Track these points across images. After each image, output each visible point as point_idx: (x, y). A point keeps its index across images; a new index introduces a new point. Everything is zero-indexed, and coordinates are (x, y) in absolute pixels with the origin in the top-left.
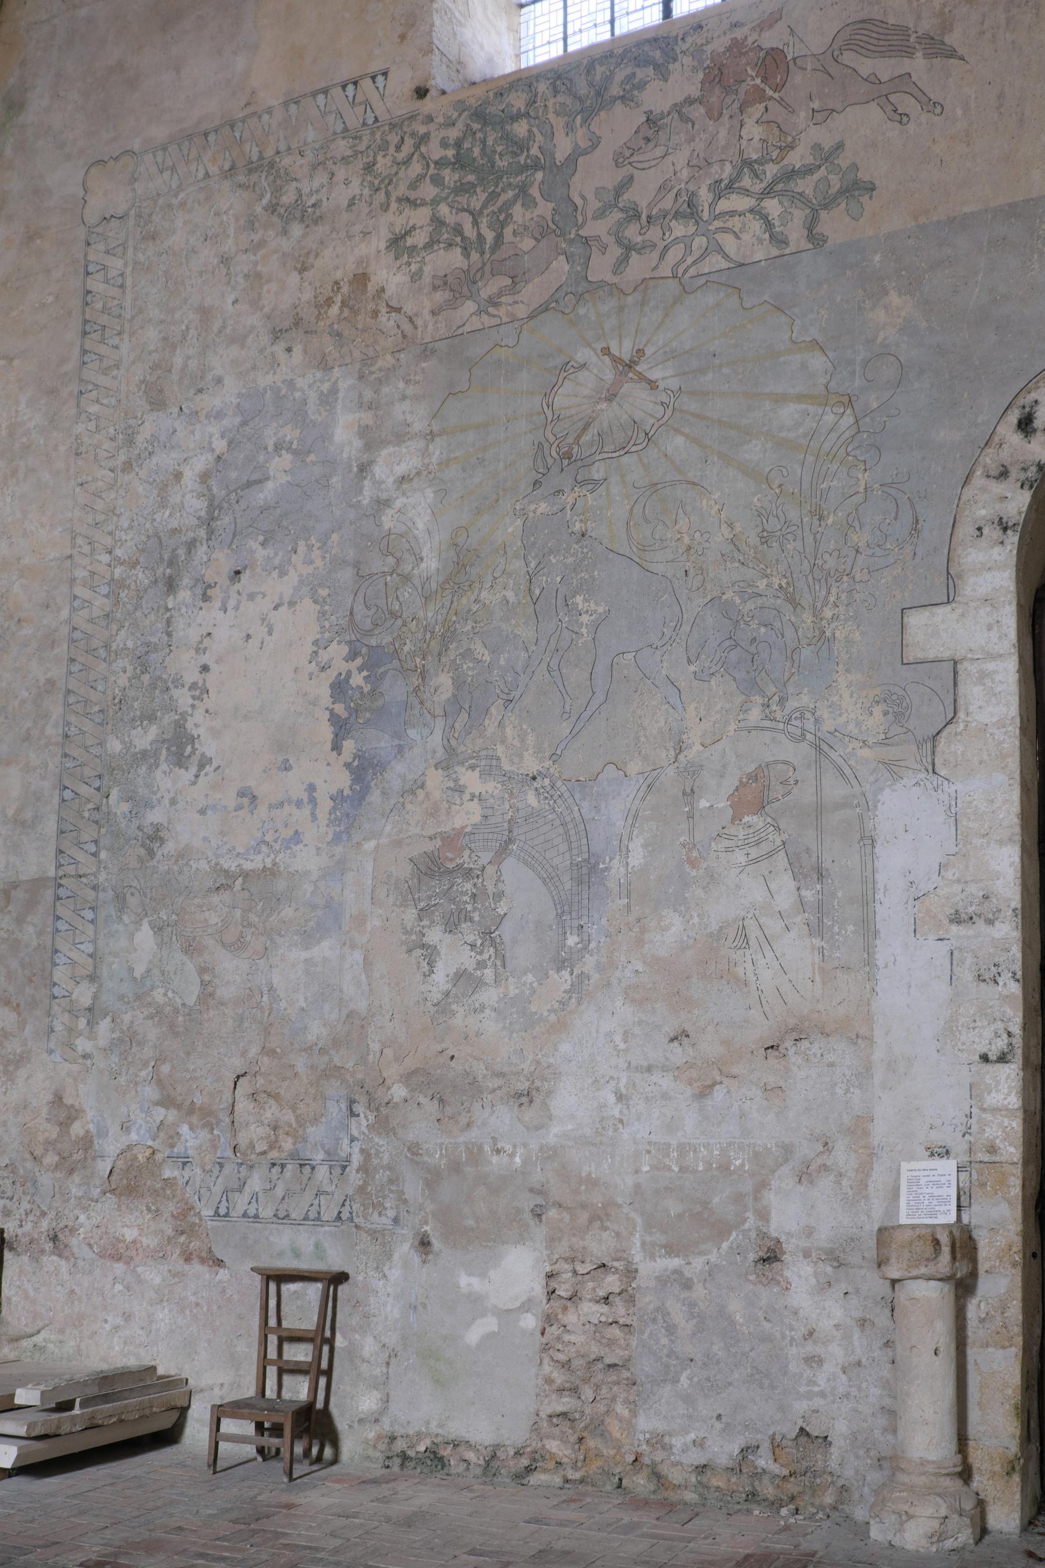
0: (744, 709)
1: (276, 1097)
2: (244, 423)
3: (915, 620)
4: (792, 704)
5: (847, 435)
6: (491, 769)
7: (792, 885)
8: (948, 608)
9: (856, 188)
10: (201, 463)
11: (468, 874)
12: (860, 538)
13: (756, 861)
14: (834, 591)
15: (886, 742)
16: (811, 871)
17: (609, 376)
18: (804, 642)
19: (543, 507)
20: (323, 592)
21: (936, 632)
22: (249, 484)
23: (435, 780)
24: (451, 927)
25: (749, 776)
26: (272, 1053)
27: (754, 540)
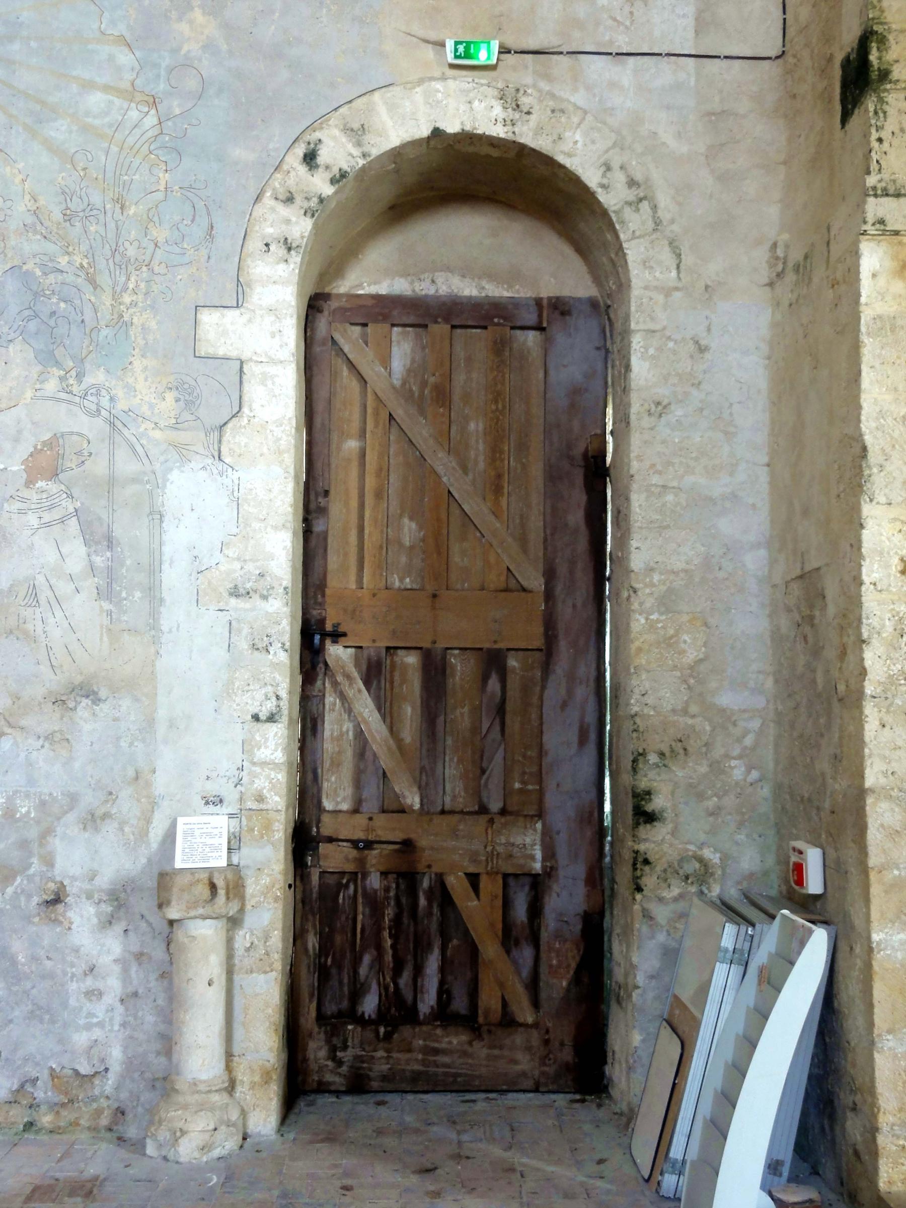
0: (42, 378)
3: (208, 318)
4: (89, 380)
5: (150, 134)
7: (83, 550)
8: (237, 312)
12: (161, 234)
13: (48, 525)
14: (133, 279)
16: (101, 539)
18: (103, 323)
21: (223, 331)
25: (44, 443)
27: (57, 216)
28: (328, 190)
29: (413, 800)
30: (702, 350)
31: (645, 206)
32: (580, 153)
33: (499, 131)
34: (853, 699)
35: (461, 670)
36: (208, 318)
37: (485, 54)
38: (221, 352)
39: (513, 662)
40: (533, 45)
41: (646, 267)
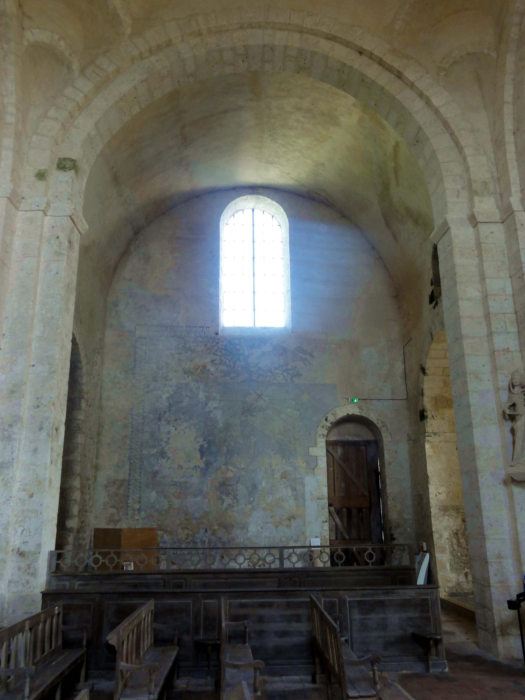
1: (187, 529)
2: (177, 389)
3: (310, 449)
4: (290, 460)
6: (235, 466)
9: (299, 375)
10: (167, 395)
11: (231, 485)
15: (306, 468)
17: (256, 397)
19: (244, 418)
20: (197, 427)
22: (179, 402)
23: (223, 467)
24: (227, 495)
26: (187, 519)
28: (330, 425)
29: (347, 537)
30: (397, 452)
31: (385, 427)
32: (373, 417)
33: (359, 414)
34: (429, 517)
35: (354, 511)
36: (310, 449)
37: (355, 401)
38: (313, 455)
39: (364, 510)
40: (363, 398)
41: (386, 438)
